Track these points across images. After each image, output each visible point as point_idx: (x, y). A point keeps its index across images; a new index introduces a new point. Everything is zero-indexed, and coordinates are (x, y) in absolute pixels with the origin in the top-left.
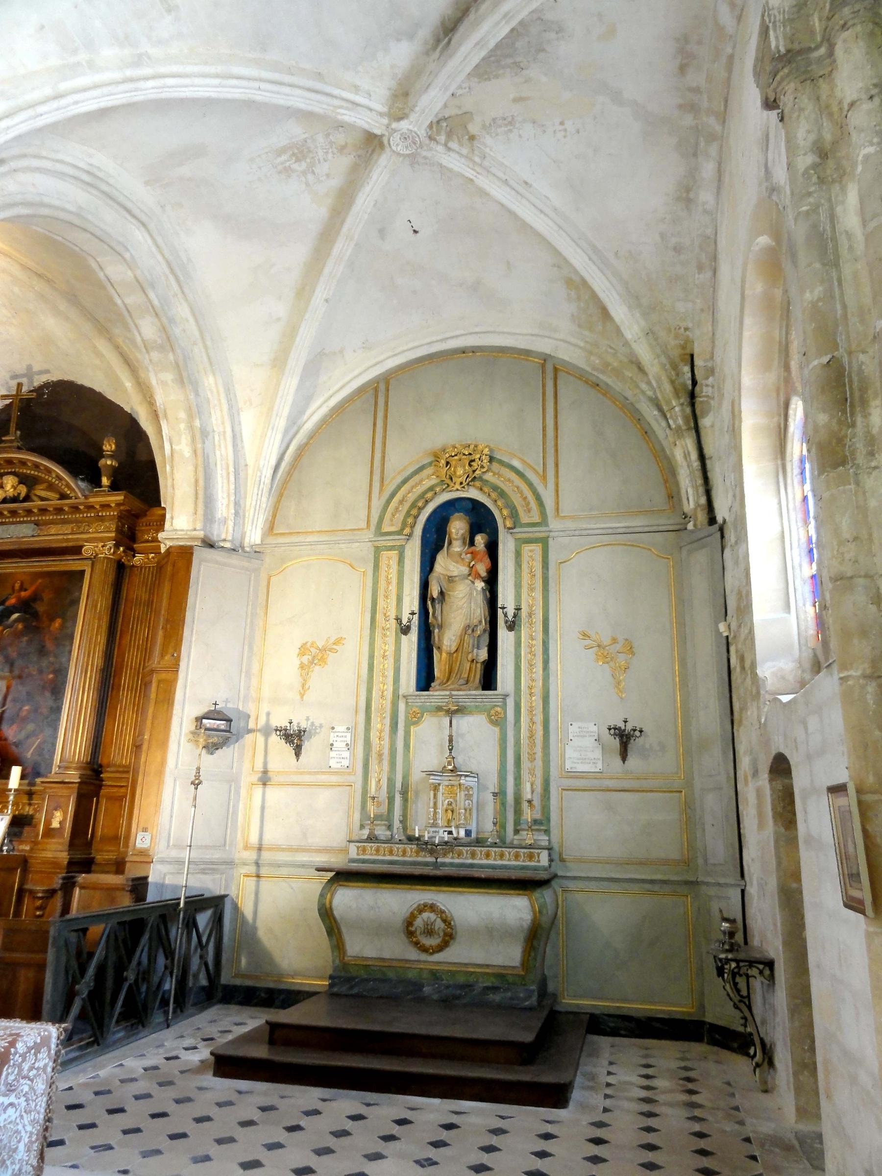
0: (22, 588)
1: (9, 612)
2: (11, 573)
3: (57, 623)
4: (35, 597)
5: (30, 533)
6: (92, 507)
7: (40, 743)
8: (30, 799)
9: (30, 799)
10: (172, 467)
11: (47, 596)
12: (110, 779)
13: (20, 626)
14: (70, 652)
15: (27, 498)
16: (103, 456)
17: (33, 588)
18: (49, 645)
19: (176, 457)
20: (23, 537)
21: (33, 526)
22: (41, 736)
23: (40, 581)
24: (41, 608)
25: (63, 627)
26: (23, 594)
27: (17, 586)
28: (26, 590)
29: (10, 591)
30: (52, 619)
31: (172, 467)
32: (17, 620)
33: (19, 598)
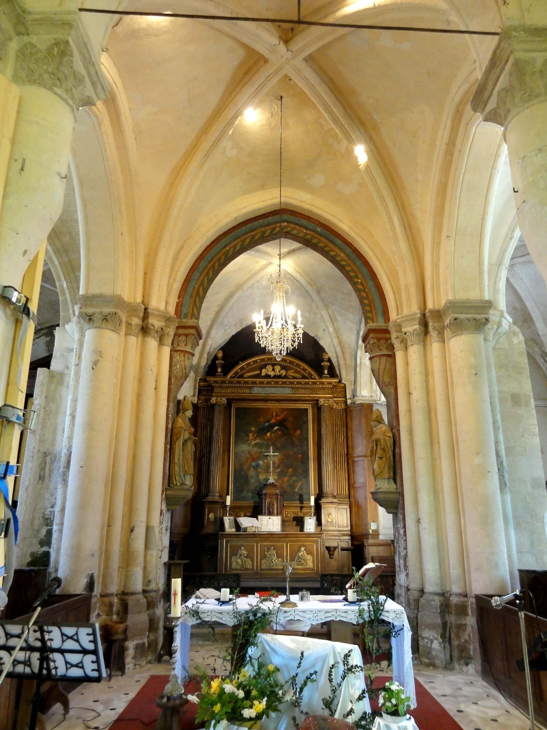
0: (277, 415)
1: (273, 426)
2: (270, 408)
3: (298, 432)
4: (284, 420)
5: (290, 392)
10: (360, 369)
11: (291, 419)
13: (280, 433)
16: (323, 361)
17: (283, 415)
18: (296, 441)
19: (362, 366)
21: (291, 389)
23: (285, 412)
24: (288, 424)
25: (301, 434)
26: (278, 418)
27: (274, 414)
28: (279, 416)
29: (271, 416)
30: (295, 430)
31: (360, 369)
33: (276, 420)
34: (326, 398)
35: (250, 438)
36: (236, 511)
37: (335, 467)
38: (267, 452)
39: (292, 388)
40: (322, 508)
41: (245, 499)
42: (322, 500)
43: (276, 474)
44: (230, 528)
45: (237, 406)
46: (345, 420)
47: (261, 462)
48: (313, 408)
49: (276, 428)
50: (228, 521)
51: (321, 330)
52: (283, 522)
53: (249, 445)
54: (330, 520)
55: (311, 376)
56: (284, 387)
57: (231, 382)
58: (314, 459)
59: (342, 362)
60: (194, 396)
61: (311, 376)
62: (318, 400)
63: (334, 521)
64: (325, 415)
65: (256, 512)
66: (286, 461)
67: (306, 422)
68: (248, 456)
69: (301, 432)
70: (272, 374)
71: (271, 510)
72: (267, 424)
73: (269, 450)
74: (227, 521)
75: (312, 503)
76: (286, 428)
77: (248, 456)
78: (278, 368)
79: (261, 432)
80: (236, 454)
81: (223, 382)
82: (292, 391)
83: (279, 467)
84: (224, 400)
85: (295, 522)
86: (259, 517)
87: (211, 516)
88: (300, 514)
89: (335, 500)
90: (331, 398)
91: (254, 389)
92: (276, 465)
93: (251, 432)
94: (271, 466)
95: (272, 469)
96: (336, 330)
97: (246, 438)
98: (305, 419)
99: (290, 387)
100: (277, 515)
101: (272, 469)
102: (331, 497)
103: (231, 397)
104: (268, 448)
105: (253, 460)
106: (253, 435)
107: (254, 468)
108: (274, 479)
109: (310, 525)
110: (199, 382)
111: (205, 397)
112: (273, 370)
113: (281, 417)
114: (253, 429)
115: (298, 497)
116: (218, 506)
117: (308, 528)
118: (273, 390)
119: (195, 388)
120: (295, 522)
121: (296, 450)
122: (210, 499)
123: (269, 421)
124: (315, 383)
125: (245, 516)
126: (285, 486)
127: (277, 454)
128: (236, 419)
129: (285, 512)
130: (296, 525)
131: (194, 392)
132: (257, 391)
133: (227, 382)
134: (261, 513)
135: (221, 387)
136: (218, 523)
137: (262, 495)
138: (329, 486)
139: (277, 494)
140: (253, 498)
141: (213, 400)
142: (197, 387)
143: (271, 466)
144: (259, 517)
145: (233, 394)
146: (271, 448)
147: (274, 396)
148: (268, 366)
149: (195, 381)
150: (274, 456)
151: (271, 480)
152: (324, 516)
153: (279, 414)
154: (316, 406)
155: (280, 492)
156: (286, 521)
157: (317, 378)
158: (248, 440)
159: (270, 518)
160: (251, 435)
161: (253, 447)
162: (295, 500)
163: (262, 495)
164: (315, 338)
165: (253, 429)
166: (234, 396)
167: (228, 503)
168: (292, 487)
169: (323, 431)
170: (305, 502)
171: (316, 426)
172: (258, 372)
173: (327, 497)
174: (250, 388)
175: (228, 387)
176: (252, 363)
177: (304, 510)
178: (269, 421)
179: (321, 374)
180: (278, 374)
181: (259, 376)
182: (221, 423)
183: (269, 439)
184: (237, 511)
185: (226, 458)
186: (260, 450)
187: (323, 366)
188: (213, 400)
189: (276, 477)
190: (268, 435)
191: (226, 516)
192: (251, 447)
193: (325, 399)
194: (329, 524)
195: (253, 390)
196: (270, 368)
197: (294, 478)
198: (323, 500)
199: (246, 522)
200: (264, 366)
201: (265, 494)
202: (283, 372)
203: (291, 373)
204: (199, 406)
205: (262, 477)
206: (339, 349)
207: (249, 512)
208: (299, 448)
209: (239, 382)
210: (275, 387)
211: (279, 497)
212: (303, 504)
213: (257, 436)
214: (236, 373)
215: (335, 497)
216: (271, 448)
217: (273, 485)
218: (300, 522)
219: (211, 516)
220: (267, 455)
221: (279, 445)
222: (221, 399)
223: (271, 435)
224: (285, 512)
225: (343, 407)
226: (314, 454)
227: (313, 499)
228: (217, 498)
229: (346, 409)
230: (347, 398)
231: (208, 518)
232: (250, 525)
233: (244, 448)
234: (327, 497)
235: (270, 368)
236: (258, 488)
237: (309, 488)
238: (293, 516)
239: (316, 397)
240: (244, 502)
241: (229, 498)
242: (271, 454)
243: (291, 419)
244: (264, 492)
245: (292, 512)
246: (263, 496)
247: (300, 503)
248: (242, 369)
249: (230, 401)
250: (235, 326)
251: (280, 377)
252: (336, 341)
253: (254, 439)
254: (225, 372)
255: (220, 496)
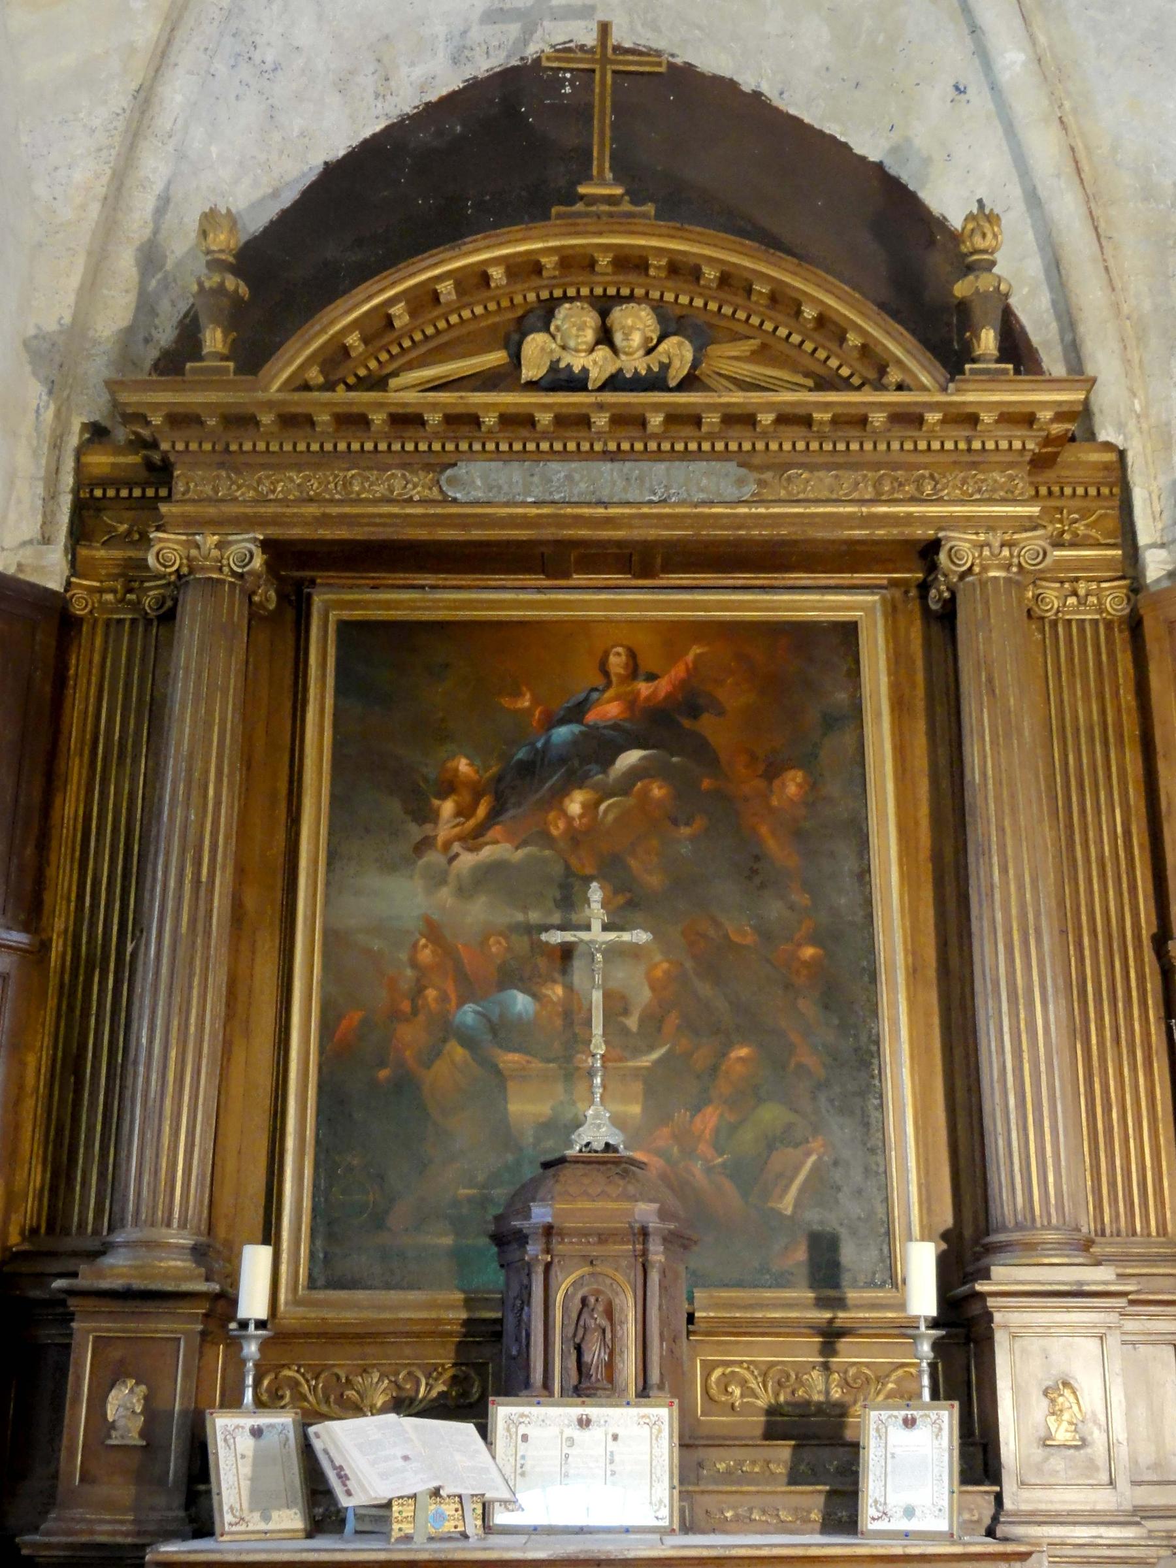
0: (634, 671)
1: (601, 747)
2: (584, 626)
3: (792, 784)
4: (690, 702)
5: (730, 491)
6: (972, 420)
7: (815, 1169)
8: (828, 1349)
9: (828, 1349)
12: (450, 1307)
14: (863, 875)
15: (690, 382)
17: (678, 672)
20: (703, 503)
21: (731, 467)
22: (816, 1144)
23: (696, 650)
26: (644, 688)
27: (617, 662)
28: (651, 677)
30: (773, 772)
32: (635, 774)
33: (631, 702)
34: (990, 525)
35: (444, 831)
36: (316, 1367)
37: (1078, 1032)
38: (562, 928)
39: (745, 461)
40: (1001, 1339)
41: (396, 1273)
42: (997, 1272)
43: (638, 1087)
44: (261, 1501)
45: (358, 614)
46: (1128, 698)
47: (521, 1002)
48: (892, 611)
49: (631, 758)
50: (246, 1444)
51: (936, 96)
52: (691, 1442)
53: (438, 879)
54: (1062, 1434)
55: (876, 368)
56: (686, 455)
57: (293, 421)
58: (913, 972)
59: (1091, 297)
60: (46, 540)
61: (876, 368)
62: (933, 547)
63: (1098, 1438)
64: (991, 647)
65: (477, 1376)
66: (705, 989)
67: (854, 715)
68: (426, 955)
69: (813, 785)
70: (597, 364)
71: (595, 1354)
72: (563, 733)
73: (575, 918)
74: (242, 1445)
75: (923, 1299)
76: (702, 751)
77: (426, 955)
78: (635, 324)
79: (520, 782)
80: (335, 941)
81: (240, 421)
82: (741, 482)
83: (653, 1022)
84: (244, 552)
85: (783, 1452)
86: (503, 1413)
87: (124, 1404)
88: (818, 1388)
89: (1101, 1276)
90: (1031, 524)
91: (462, 470)
92: (632, 1022)
93: (448, 788)
94: (598, 1029)
95: (599, 1047)
96: (1050, 70)
97: (416, 832)
98: (842, 696)
99: (726, 455)
100: (644, 1392)
101: (599, 1047)
102: (1061, 1247)
103: (296, 533)
104: (569, 899)
105: (469, 989)
106: (463, 812)
107: (468, 1041)
108: (618, 1122)
109: (908, 1467)
110: (79, 453)
111: (117, 554)
112: (605, 337)
113: (663, 686)
114: (463, 766)
115: (801, 1254)
116: (181, 1326)
117: (896, 1500)
118: (608, 478)
119: (52, 496)
120: (783, 1452)
121: (774, 909)
122: (118, 1269)
123: (576, 713)
124: (909, 419)
125: (402, 1405)
126: (698, 1167)
127: (640, 936)
128: (339, 691)
129: (709, 1367)
130: (794, 1478)
131: (48, 521)
132: (496, 489)
133: (266, 419)
134: (515, 1383)
135: (226, 460)
136: (175, 1465)
137: (522, 1239)
138: (1038, 1164)
139: (645, 1233)
140: (461, 1258)
141: (167, 550)
142: (68, 480)
143: (598, 1029)
144: (503, 1413)
145: (312, 510)
146: (596, 893)
147: (608, 521)
148: (563, 311)
149: (57, 445)
150: (614, 952)
151: (597, 1129)
152: (1016, 1389)
153: (648, 662)
154: (915, 607)
155: (663, 1214)
156: (719, 1441)
157: (925, 379)
158: (426, 843)
159: (584, 1423)
160: (447, 808)
161: (465, 891)
162: (782, 1281)
163: (522, 1239)
164: (893, 169)
165: (463, 766)
166: (324, 520)
167: (253, 1302)
168: (751, 1175)
169: (982, 758)
170: (852, 1295)
171: (920, 743)
172: (497, 358)
173: (1029, 1250)
174: (439, 465)
175: (277, 463)
176: (446, 289)
177: (849, 1354)
178: (576, 713)
179: (953, 358)
180: (635, 363)
181: (505, 377)
182: (226, 711)
183: (576, 838)
184: (341, 1363)
185: (266, 972)
186: (520, 917)
187: (963, 308)
188: (167, 550)
189: (635, 1109)
190: (575, 805)
191: (232, 1401)
192: (445, 894)
193: (986, 528)
194: (1057, 1463)
195: (451, 481)
196: (576, 323)
197: (771, 1115)
198: (1004, 1275)
199: (385, 1455)
200: (543, 315)
201: (548, 1231)
202: (678, 353)
203: (728, 358)
204: (79, 609)
205: (526, 1107)
206: (1066, 207)
207: (431, 1372)
208: (802, 899)
209: (354, 421)
210: (615, 456)
211: (657, 1253)
212: (839, 1303)
213: (494, 815)
214: (335, 357)
215: (1084, 1248)
216: (596, 893)
217: (607, 1161)
218: (821, 1448)
219: (124, 1404)
220: (566, 952)
221: (654, 881)
222: (220, 546)
223: (590, 808)
224: (709, 1367)
225: (1114, 600)
226: (914, 931)
227: (921, 1266)
228: (174, 1267)
229: (1134, 625)
230: (1143, 539)
231: (100, 1424)
232: (420, 1484)
233: (402, 899)
234: (1030, 1247)
235: (576, 323)
236: (500, 1193)
237: (885, 1188)
238: (763, 1401)
239: (924, 520)
240: (394, 1296)
241: (256, 1262)
242: (597, 935)
243: (734, 696)
244: (541, 1214)
245: (757, 1369)
246: (534, 1249)
247: (821, 1303)
248: (380, 325)
249: (296, 564)
250: (342, 85)
251: (655, 382)
252: (1045, 148)
253: (474, 839)
254: (252, 356)
255: (199, 1253)
